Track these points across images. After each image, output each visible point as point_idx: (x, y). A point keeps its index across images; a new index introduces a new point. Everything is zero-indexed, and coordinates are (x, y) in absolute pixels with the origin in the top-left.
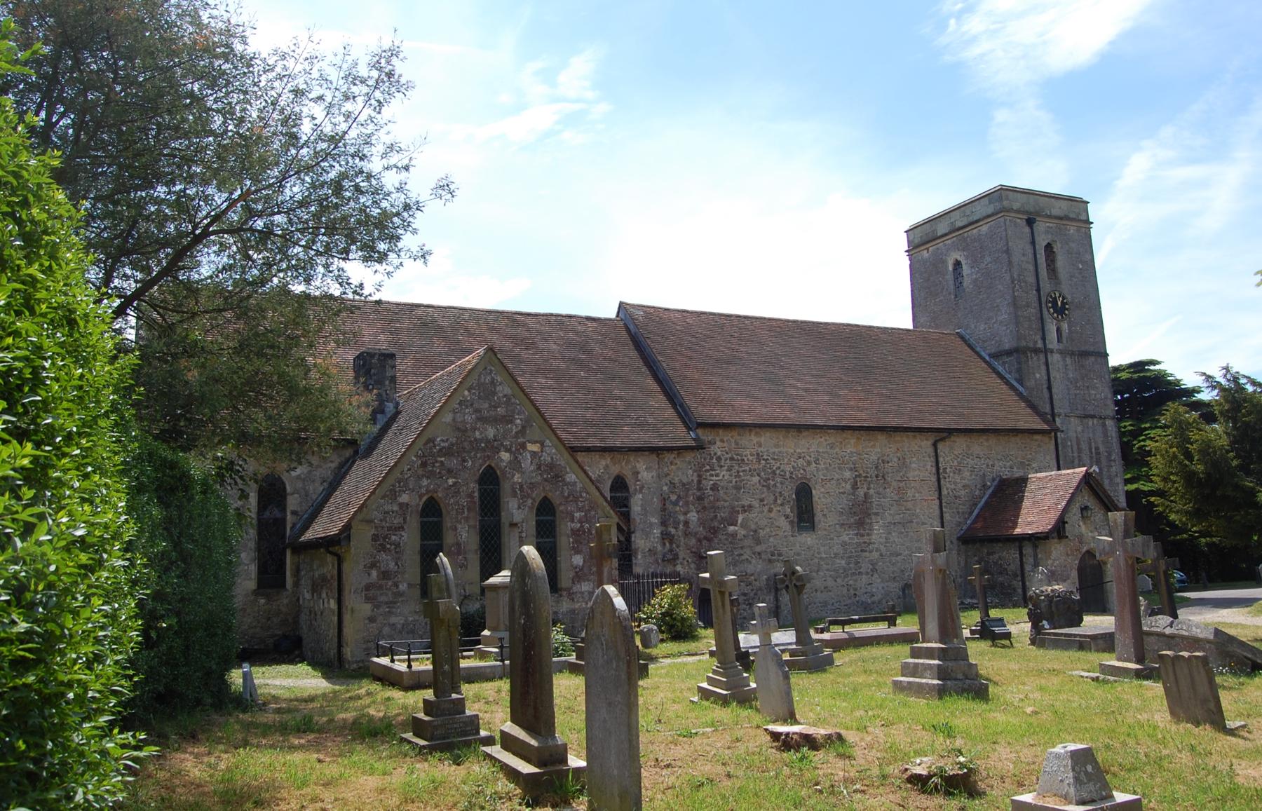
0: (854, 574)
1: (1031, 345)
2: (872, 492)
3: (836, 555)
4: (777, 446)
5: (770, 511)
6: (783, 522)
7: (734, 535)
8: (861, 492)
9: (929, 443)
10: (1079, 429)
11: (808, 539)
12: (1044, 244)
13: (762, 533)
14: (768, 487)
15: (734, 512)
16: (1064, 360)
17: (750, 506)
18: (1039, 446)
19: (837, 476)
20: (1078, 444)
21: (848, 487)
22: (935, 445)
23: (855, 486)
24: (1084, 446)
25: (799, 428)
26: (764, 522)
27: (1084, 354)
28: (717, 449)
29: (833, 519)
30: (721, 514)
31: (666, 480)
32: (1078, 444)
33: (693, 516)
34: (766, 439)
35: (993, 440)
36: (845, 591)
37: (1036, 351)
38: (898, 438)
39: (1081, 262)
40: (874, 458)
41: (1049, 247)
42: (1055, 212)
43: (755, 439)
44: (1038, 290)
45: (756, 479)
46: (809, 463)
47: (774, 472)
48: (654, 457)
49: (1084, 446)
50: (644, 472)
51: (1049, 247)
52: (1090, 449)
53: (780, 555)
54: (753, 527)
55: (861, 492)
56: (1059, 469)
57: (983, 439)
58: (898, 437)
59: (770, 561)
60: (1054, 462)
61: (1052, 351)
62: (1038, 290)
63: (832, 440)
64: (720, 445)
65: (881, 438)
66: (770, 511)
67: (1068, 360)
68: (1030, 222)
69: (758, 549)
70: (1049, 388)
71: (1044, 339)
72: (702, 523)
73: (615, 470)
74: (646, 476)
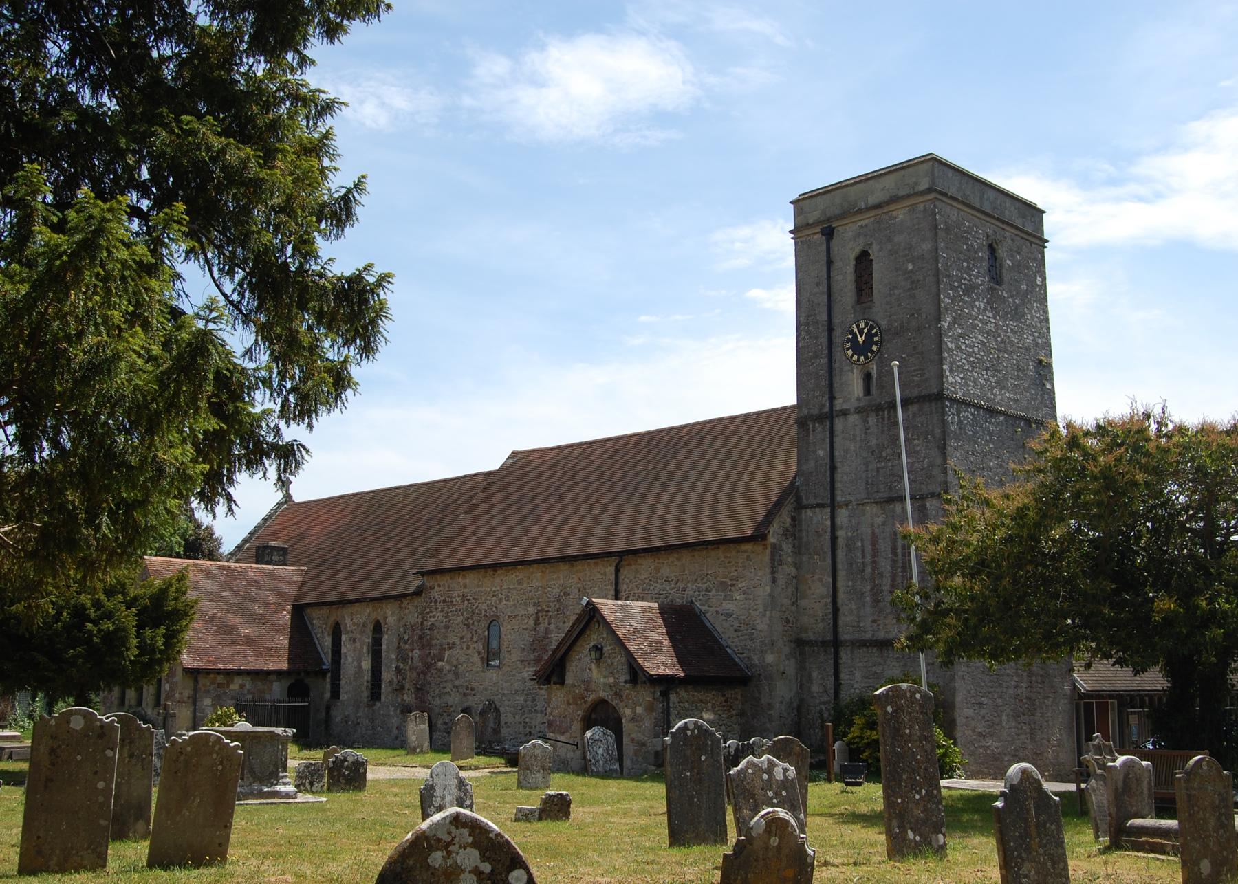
0: (530, 712)
1: (815, 411)
2: (552, 626)
3: (517, 691)
4: (478, 586)
5: (468, 648)
6: (476, 659)
7: (441, 670)
8: (541, 628)
9: (611, 570)
10: (879, 521)
11: (493, 675)
12: (853, 256)
13: (461, 668)
14: (468, 626)
15: (442, 649)
16: (865, 421)
17: (454, 644)
18: (748, 558)
19: (523, 613)
20: (874, 543)
21: (531, 622)
22: (617, 571)
23: (537, 622)
24: (884, 546)
25: (494, 567)
26: (462, 659)
27: (922, 399)
28: (435, 593)
29: (516, 655)
30: (435, 651)
31: (402, 623)
32: (874, 543)
33: (416, 653)
34: (471, 579)
35: (686, 557)
36: (522, 729)
37: (820, 418)
38: (580, 567)
39: (912, 261)
40: (556, 591)
41: (863, 260)
42: (872, 200)
43: (461, 581)
44: (830, 329)
45: (460, 619)
46: (500, 601)
47: (473, 612)
48: (397, 604)
49: (884, 546)
50: (390, 615)
51: (863, 260)
52: (895, 553)
53: (473, 689)
54: (455, 663)
55: (541, 628)
56: (617, 599)
57: (673, 558)
58: (579, 566)
59: (464, 694)
60: (612, 592)
61: (845, 413)
62: (830, 329)
63: (521, 576)
64: (439, 589)
65: (564, 568)
66: (468, 648)
67: (872, 420)
68: (829, 233)
69: (457, 683)
70: (833, 468)
71: (832, 398)
72: (421, 659)
73: (374, 616)
74: (391, 620)
